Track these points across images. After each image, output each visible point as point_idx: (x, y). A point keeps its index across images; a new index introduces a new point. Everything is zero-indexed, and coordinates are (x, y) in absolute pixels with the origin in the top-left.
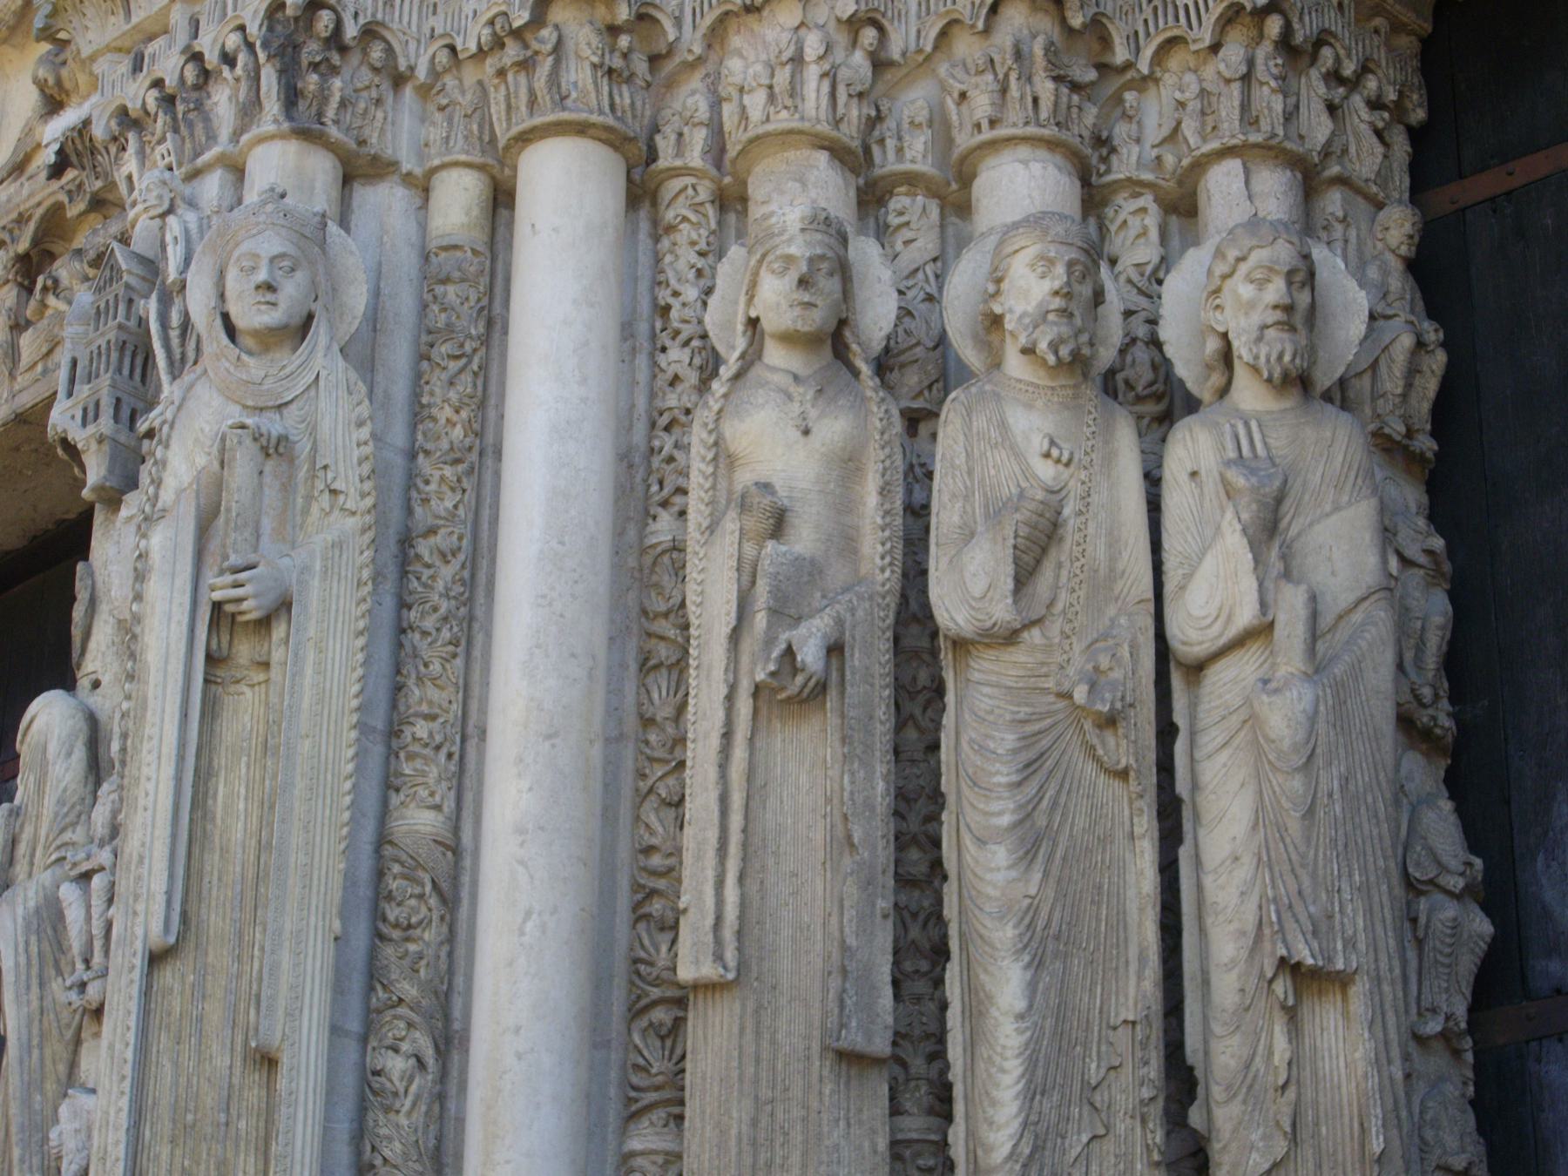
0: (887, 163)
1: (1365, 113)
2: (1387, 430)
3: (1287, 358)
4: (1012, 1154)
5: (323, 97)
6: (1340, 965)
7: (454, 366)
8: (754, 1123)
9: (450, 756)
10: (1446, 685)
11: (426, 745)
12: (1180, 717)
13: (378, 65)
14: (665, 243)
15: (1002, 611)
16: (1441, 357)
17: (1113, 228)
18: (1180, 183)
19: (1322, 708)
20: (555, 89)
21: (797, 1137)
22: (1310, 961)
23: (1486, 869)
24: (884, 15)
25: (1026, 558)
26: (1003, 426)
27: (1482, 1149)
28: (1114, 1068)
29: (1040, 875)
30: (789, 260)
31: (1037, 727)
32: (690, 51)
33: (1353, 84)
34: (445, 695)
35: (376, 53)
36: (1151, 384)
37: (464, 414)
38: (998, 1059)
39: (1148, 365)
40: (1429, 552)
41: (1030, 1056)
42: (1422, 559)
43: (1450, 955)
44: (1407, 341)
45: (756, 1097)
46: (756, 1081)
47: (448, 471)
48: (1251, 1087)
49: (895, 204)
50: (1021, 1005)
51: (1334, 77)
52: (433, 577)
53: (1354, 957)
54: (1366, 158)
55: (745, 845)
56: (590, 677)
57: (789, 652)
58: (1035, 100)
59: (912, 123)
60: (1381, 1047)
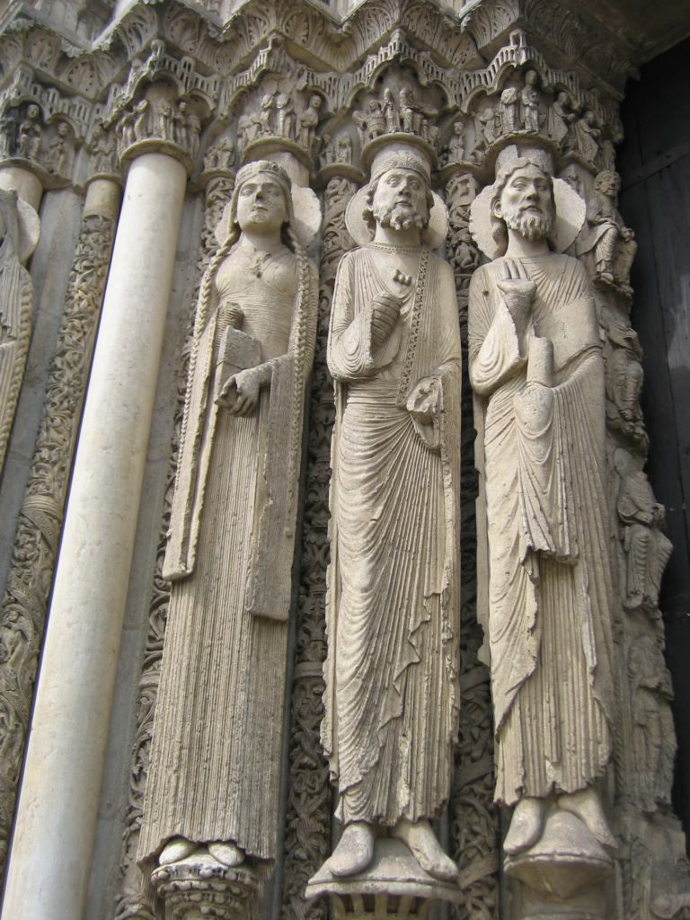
0: (327, 164)
1: (587, 129)
2: (603, 279)
3: (536, 224)
4: (356, 673)
5: (28, 146)
6: (567, 553)
8: (199, 659)
9: (62, 469)
10: (641, 413)
11: (47, 462)
13: (62, 134)
14: (208, 210)
15: (366, 359)
16: (633, 245)
17: (450, 191)
18: (486, 165)
19: (556, 404)
20: (144, 129)
21: (224, 667)
22: (547, 548)
23: (667, 511)
24: (324, 90)
27: (669, 676)
28: (427, 622)
30: (252, 187)
31: (384, 425)
32: (222, 115)
33: (581, 114)
34: (61, 436)
35: (62, 128)
36: (469, 263)
37: (89, 296)
39: (468, 253)
40: (628, 340)
41: (370, 614)
42: (624, 343)
43: (644, 553)
44: (612, 232)
45: (201, 644)
46: (202, 634)
47: (76, 322)
48: (513, 630)
49: (331, 184)
50: (366, 582)
51: (567, 108)
52: (62, 376)
53: (576, 547)
54: (589, 150)
55: (205, 497)
56: (135, 418)
57: (234, 385)
59: (340, 145)
60: (595, 603)
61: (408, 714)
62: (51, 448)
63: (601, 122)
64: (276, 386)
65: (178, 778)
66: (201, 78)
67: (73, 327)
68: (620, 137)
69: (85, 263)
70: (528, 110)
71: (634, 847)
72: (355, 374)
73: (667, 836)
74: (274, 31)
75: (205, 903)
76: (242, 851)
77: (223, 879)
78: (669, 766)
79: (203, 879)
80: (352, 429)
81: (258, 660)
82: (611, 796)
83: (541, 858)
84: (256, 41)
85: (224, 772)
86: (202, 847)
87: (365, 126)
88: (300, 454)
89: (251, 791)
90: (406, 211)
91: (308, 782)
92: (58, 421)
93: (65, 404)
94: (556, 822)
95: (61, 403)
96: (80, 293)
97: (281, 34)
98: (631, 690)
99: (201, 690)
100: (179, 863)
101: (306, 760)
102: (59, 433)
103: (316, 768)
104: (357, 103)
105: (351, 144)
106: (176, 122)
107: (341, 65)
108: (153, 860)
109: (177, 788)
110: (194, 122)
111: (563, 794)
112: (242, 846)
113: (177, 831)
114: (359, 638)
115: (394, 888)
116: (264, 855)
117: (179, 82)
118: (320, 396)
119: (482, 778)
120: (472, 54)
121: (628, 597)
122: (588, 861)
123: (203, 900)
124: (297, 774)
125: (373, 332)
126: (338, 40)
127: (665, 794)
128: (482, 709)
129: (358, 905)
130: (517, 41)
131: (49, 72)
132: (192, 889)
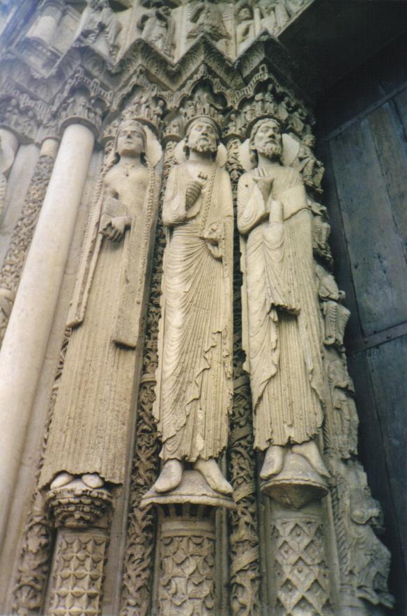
1: (298, 116)
7: (39, 181)
8: (83, 368)
11: (8, 272)
12: (242, 250)
15: (182, 212)
16: (322, 169)
21: (98, 372)
23: (346, 293)
25: (190, 199)
26: (187, 170)
29: (189, 286)
30: (126, 132)
33: (295, 109)
35: (30, 113)
37: (40, 192)
38: (170, 342)
40: (322, 211)
41: (182, 341)
42: (319, 213)
44: (312, 161)
45: (85, 359)
46: (86, 354)
48: (263, 350)
49: (169, 143)
51: (288, 104)
54: (299, 126)
55: (92, 282)
58: (204, 110)
60: (311, 335)
61: (203, 397)
62: (11, 265)
63: (305, 114)
64: (134, 227)
65: (66, 436)
66: (103, 91)
67: (29, 207)
68: (314, 123)
69: (38, 177)
70: (268, 103)
71: (338, 479)
72: (177, 220)
73: (357, 474)
74: (141, 65)
75: (78, 512)
76: (103, 479)
77: (89, 497)
78: (355, 432)
79: (77, 496)
80: (176, 250)
81: (118, 368)
82: (322, 449)
83: (284, 482)
84: (131, 72)
85: (94, 432)
86: (78, 477)
87: (186, 114)
88: (146, 262)
89: (110, 442)
90: (205, 143)
91: (146, 440)
92: (16, 252)
93: (22, 244)
94: (292, 459)
95: (19, 243)
96: (35, 191)
97: (143, 66)
98: (330, 389)
99: (83, 385)
100: (62, 488)
101: (146, 427)
102: (17, 257)
103: (151, 432)
104: (182, 105)
105: (179, 125)
106: (89, 110)
107: (175, 88)
108: (47, 487)
109: (65, 442)
110: (99, 111)
111: (296, 444)
112: (102, 476)
113: (63, 468)
114: (176, 353)
115: (194, 500)
116: (116, 481)
117: (91, 90)
118: (160, 235)
119: (245, 437)
120: (240, 81)
121: (326, 339)
122: (314, 484)
123: (76, 510)
124: (140, 436)
125: (187, 200)
126: (173, 74)
127: (354, 448)
128: (245, 399)
129: (172, 510)
130: (263, 69)
131: (25, 85)
132: (69, 504)
